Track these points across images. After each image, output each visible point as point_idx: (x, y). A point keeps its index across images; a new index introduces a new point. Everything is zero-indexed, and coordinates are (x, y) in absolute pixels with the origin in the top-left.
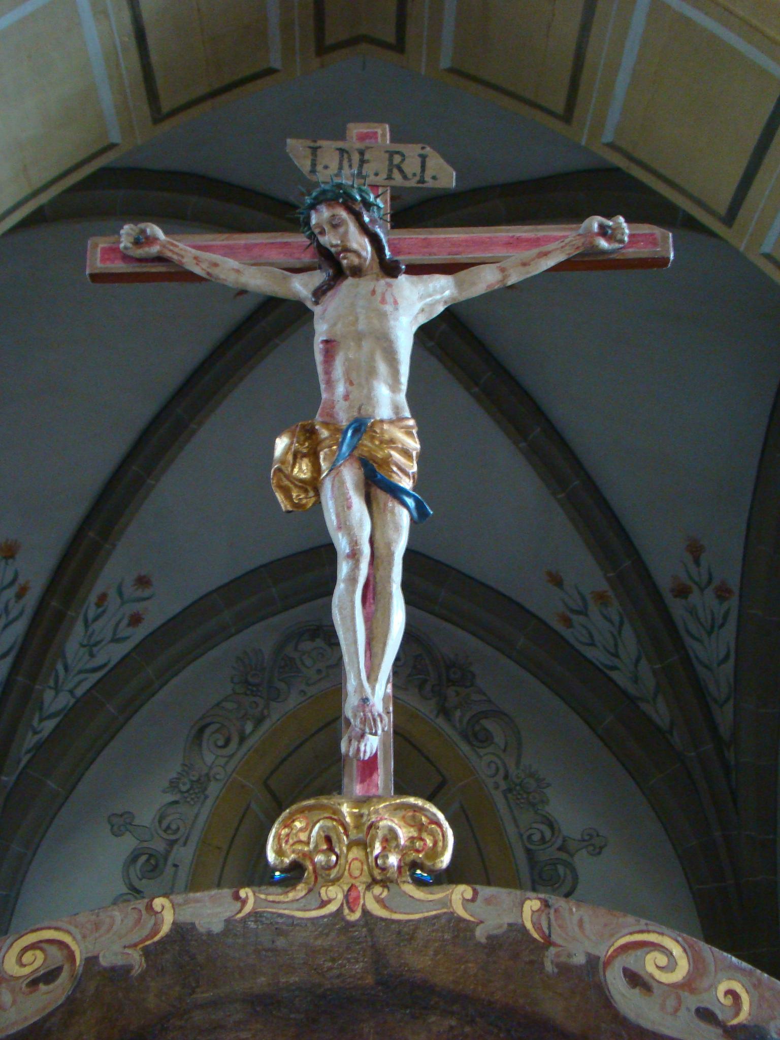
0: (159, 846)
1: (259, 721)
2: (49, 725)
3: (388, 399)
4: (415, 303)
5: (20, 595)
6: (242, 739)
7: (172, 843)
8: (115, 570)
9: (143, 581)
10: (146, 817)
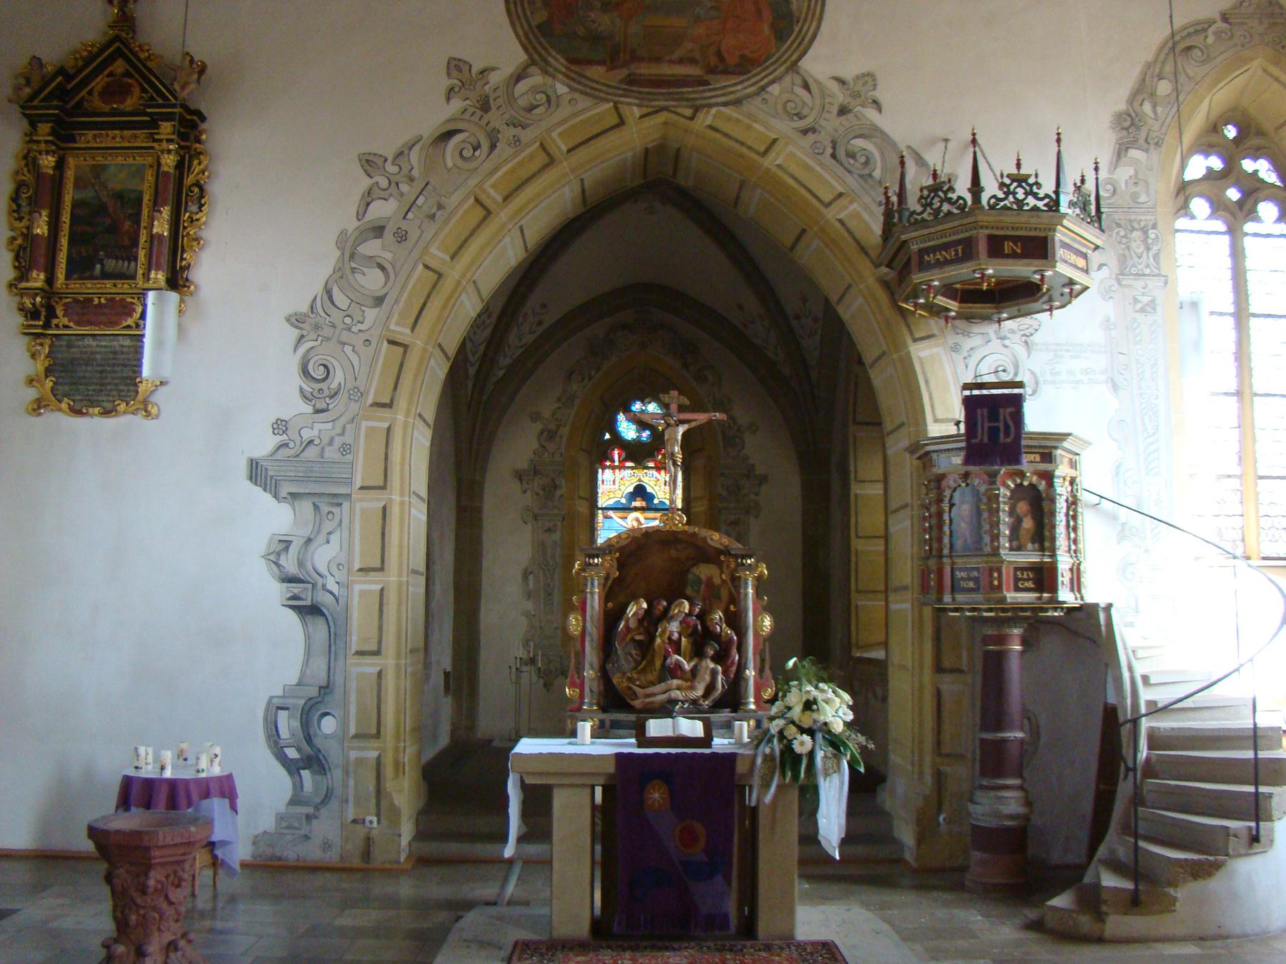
0: (552, 427)
1: (598, 369)
2: (501, 373)
3: (677, 449)
4: (681, 430)
5: (489, 317)
6: (590, 378)
7: (559, 426)
8: (533, 301)
9: (544, 306)
10: (546, 414)
